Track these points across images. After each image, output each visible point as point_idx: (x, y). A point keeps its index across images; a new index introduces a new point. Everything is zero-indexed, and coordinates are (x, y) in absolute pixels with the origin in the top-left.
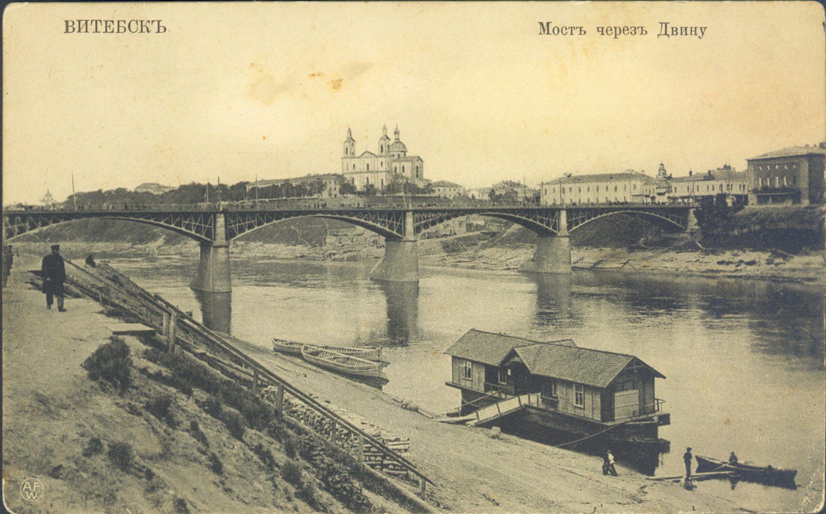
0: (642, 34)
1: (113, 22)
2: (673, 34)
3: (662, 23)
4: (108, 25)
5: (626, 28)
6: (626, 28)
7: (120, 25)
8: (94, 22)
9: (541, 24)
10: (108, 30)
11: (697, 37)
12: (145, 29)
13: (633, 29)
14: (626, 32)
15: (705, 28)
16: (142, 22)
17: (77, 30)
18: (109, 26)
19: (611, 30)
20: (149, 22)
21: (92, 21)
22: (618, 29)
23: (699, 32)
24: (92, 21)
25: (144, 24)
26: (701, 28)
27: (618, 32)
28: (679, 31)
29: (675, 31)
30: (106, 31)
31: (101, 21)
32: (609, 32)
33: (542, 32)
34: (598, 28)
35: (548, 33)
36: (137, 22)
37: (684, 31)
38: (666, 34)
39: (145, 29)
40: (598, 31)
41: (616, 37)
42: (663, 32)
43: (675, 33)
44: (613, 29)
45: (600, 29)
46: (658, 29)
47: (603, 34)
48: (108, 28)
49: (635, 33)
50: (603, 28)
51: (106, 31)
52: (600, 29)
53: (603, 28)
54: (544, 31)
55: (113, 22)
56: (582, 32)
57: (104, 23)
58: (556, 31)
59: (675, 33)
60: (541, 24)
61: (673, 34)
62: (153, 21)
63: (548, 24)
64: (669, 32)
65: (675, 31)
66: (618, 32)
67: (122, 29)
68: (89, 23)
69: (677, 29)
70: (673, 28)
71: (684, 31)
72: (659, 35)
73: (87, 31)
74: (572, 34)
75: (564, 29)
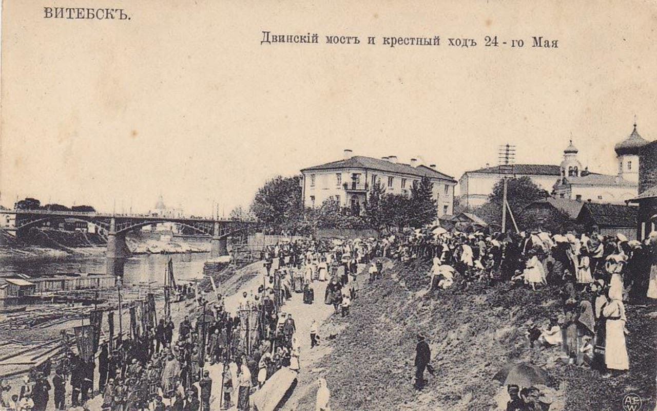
1: (83, 9)
3: (264, 32)
4: (80, 12)
8: (68, 10)
10: (80, 16)
12: (109, 16)
16: (107, 10)
17: (54, 15)
18: (81, 13)
20: (113, 10)
21: (67, 9)
24: (67, 9)
25: (109, 11)
29: (275, 39)
30: (78, 18)
31: (73, 9)
36: (103, 10)
38: (268, 41)
39: (109, 16)
42: (266, 40)
48: (80, 15)
55: (83, 9)
57: (76, 10)
61: (273, 41)
62: (116, 10)
64: (270, 39)
65: (275, 39)
67: (91, 16)
68: (64, 10)
70: (273, 36)
73: (62, 17)
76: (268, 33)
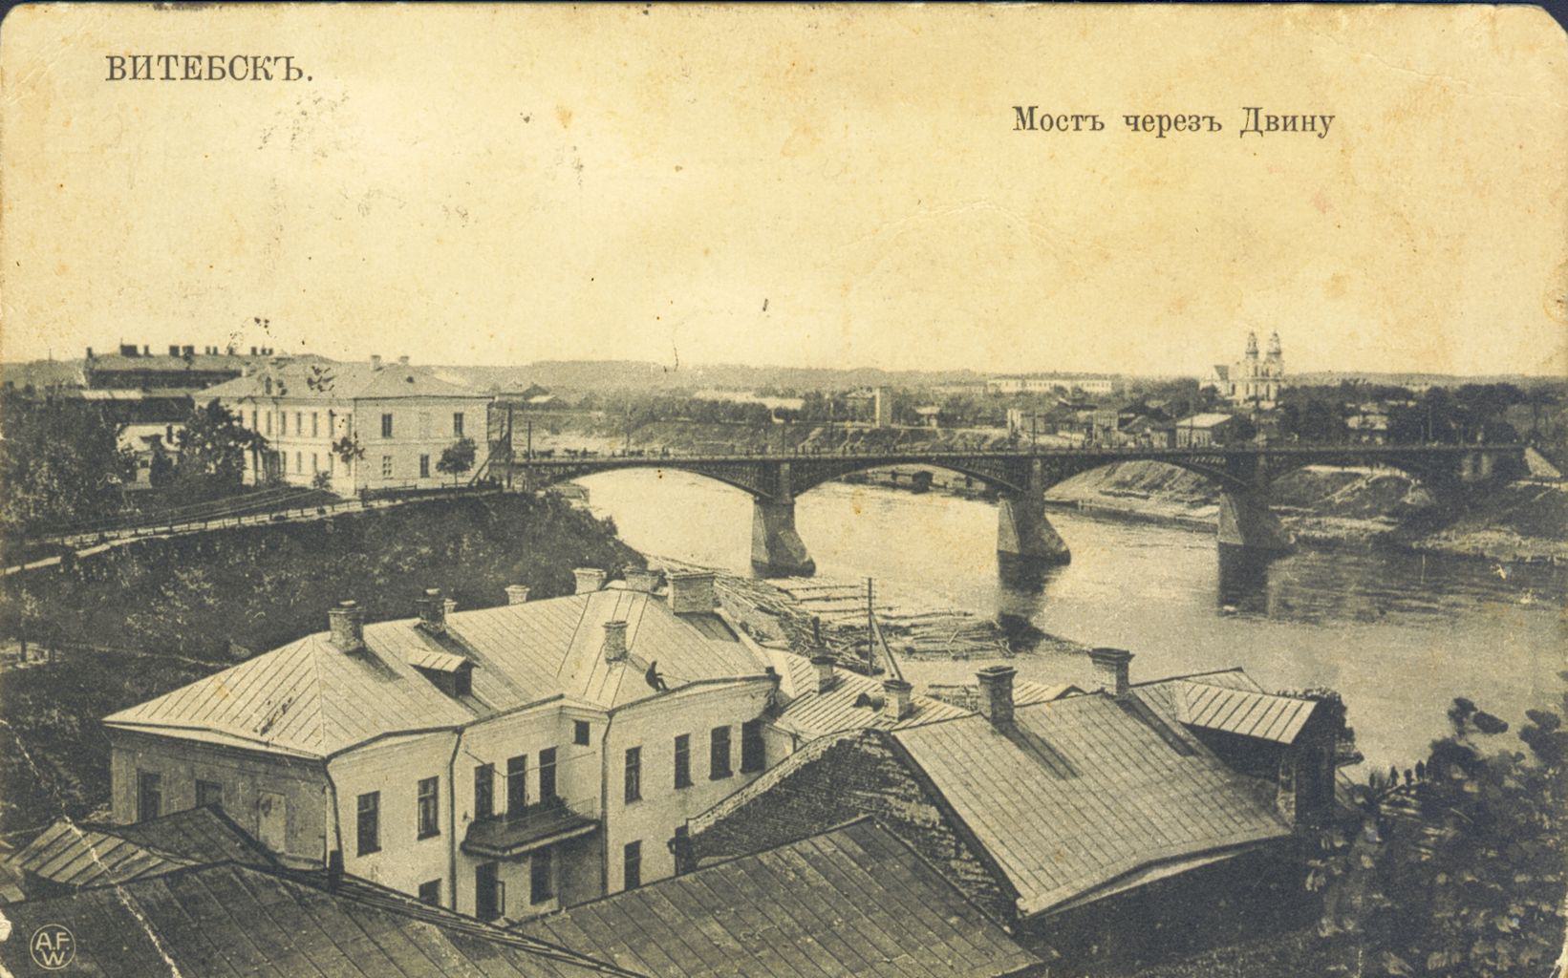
0: (1211, 129)
1: (199, 58)
2: (1269, 129)
3: (1249, 109)
4: (191, 64)
5: (1180, 119)
6: (1180, 119)
7: (214, 65)
8: (163, 60)
9: (1019, 110)
10: (191, 75)
11: (1315, 134)
13: (1194, 119)
14: (1180, 126)
15: (1331, 117)
18: (193, 67)
19: (1152, 121)
22: (1165, 120)
23: (1318, 122)
24: (160, 57)
26: (1323, 118)
27: (1165, 125)
28: (1281, 122)
29: (1273, 123)
30: (187, 77)
31: (176, 57)
32: (1149, 126)
33: (1021, 126)
34: (1127, 118)
35: (1032, 128)
37: (1290, 123)
38: (1256, 129)
40: (1128, 123)
41: (1161, 135)
42: (1251, 126)
43: (1273, 127)
44: (1157, 120)
45: (1132, 120)
46: (1242, 119)
47: (1136, 129)
48: (191, 71)
49: (1199, 127)
50: (1136, 118)
51: (187, 77)
52: (1132, 120)
53: (1136, 118)
54: (1024, 123)
55: (199, 58)
56: (1097, 126)
57: (182, 61)
58: (1047, 121)
59: (1273, 127)
60: (1019, 110)
61: (1269, 129)
63: (1031, 109)
64: (1263, 126)
65: (1273, 123)
66: (1165, 125)
67: (217, 73)
69: (1277, 119)
70: (1268, 118)
71: (1290, 123)
72: (1242, 132)
74: (1077, 129)
75: (1062, 119)
76: (1256, 110)
